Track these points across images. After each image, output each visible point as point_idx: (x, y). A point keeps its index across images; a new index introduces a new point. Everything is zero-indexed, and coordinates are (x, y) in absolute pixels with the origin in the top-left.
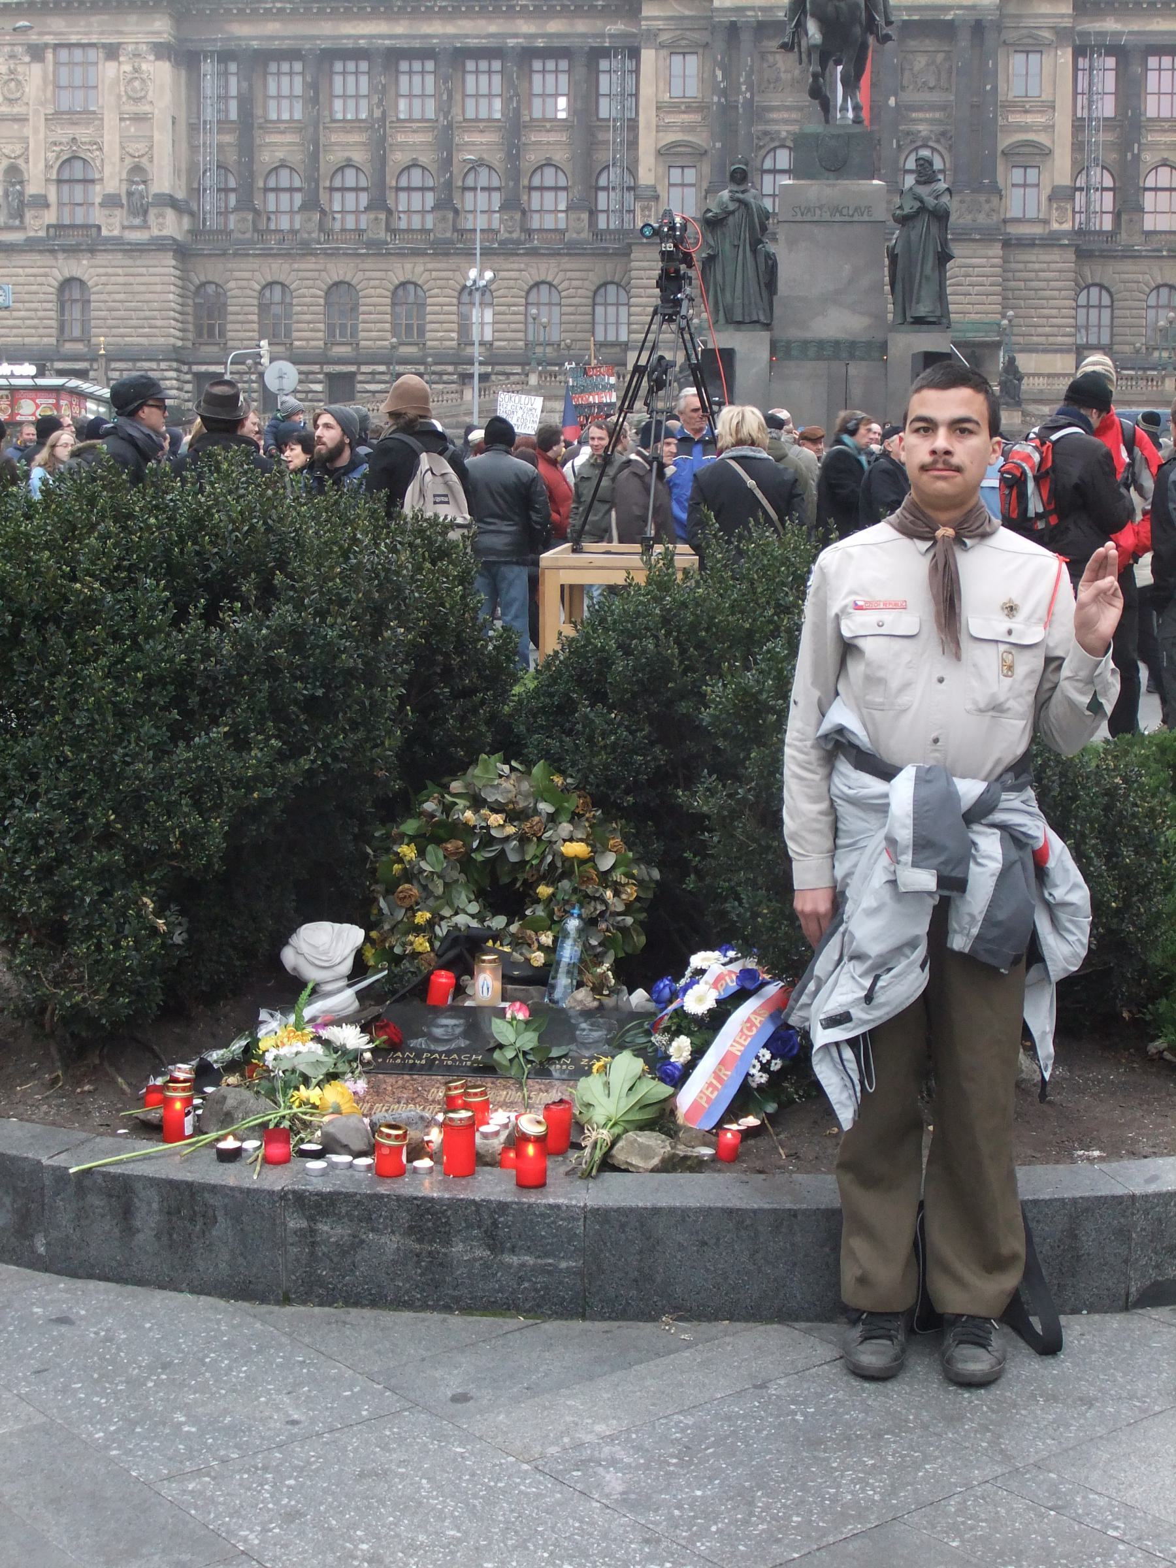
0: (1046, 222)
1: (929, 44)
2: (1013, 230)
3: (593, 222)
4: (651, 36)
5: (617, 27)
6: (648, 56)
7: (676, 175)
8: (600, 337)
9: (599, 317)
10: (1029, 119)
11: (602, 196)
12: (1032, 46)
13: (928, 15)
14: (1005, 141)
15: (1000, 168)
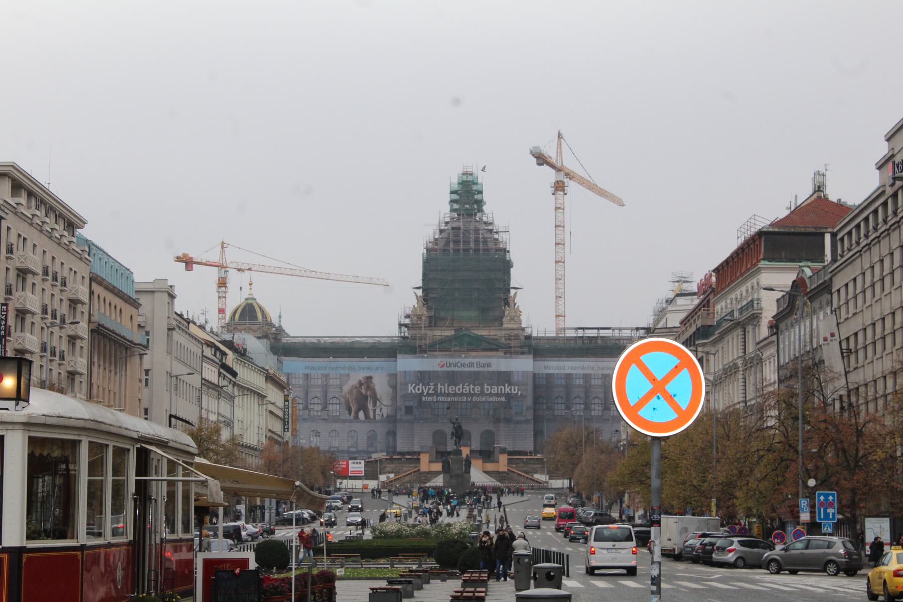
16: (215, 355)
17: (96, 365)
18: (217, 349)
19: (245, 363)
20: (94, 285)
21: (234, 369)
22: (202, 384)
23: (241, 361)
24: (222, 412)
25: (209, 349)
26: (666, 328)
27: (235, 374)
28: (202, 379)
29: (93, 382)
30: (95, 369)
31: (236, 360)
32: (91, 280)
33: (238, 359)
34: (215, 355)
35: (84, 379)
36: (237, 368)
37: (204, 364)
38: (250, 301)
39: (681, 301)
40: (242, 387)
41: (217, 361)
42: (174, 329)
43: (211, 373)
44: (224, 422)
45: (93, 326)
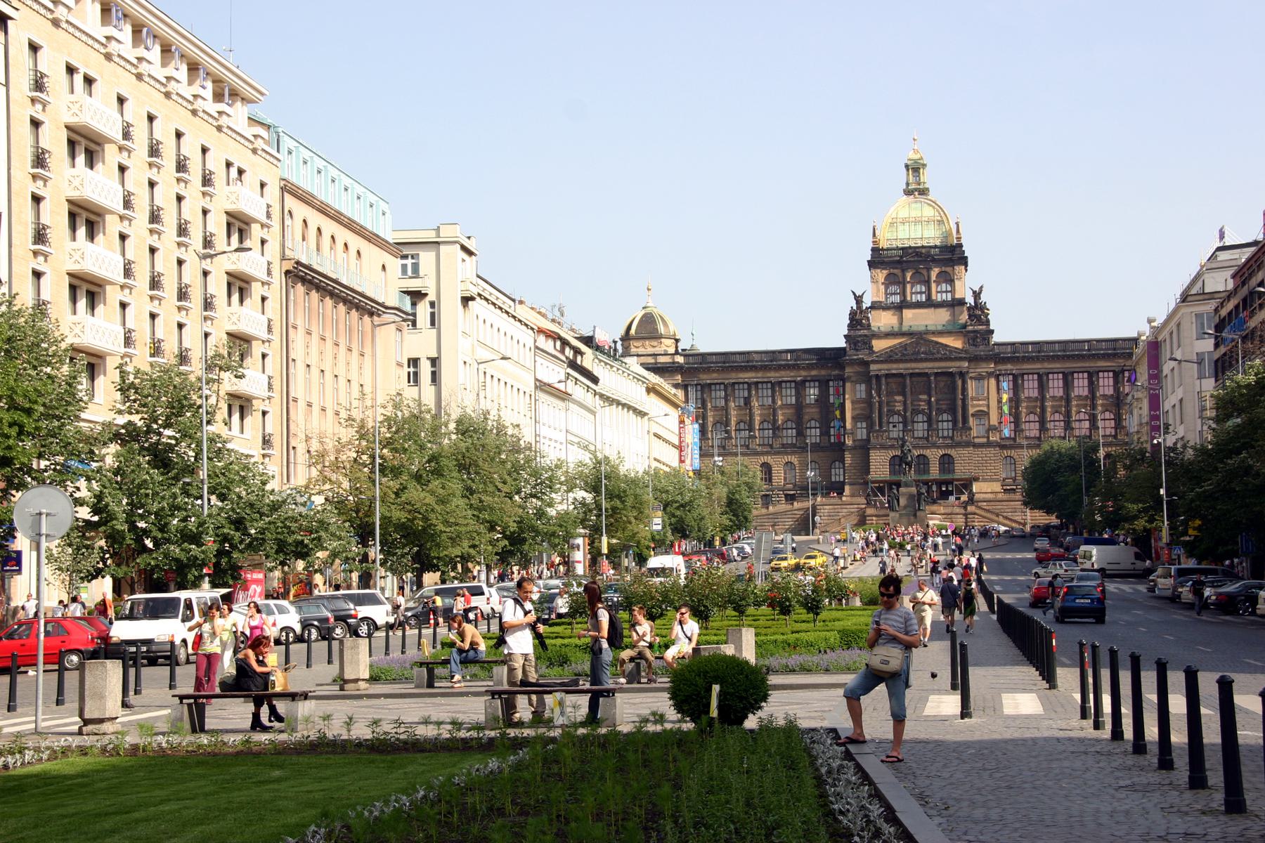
0: (988, 438)
1: (944, 378)
2: (977, 440)
3: (829, 440)
4: (849, 378)
5: (836, 372)
6: (848, 385)
7: (859, 425)
8: (833, 480)
9: (833, 473)
10: (981, 402)
11: (832, 430)
12: (980, 378)
13: (944, 370)
14: (971, 411)
15: (971, 419)
16: (562, 351)
17: (301, 331)
18: (565, 343)
19: (612, 367)
20: (290, 202)
21: (596, 373)
22: (536, 387)
23: (606, 364)
24: (574, 431)
25: (551, 342)
26: (1204, 293)
27: (595, 380)
28: (537, 380)
29: (292, 356)
30: (298, 338)
31: (596, 361)
32: (283, 189)
33: (600, 361)
34: (562, 351)
35: (274, 351)
36: (597, 370)
37: (537, 358)
38: (648, 310)
39: (1223, 256)
40: (608, 398)
41: (564, 359)
42: (472, 299)
43: (554, 373)
44: (579, 443)
45: (288, 266)
